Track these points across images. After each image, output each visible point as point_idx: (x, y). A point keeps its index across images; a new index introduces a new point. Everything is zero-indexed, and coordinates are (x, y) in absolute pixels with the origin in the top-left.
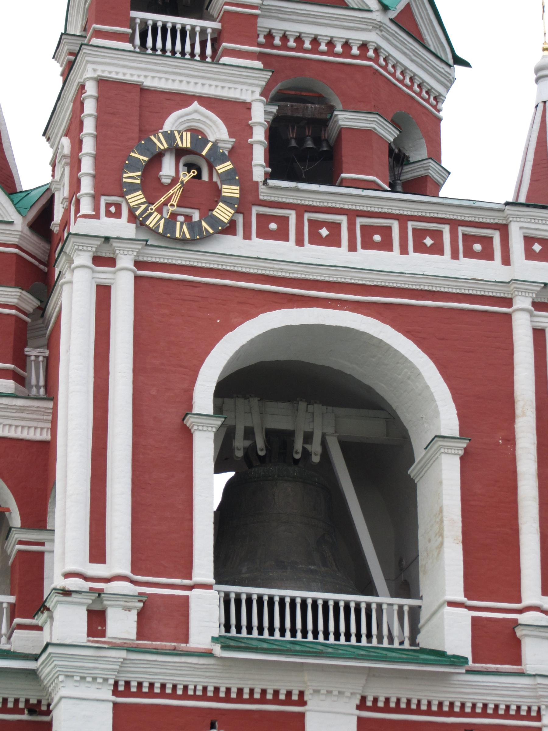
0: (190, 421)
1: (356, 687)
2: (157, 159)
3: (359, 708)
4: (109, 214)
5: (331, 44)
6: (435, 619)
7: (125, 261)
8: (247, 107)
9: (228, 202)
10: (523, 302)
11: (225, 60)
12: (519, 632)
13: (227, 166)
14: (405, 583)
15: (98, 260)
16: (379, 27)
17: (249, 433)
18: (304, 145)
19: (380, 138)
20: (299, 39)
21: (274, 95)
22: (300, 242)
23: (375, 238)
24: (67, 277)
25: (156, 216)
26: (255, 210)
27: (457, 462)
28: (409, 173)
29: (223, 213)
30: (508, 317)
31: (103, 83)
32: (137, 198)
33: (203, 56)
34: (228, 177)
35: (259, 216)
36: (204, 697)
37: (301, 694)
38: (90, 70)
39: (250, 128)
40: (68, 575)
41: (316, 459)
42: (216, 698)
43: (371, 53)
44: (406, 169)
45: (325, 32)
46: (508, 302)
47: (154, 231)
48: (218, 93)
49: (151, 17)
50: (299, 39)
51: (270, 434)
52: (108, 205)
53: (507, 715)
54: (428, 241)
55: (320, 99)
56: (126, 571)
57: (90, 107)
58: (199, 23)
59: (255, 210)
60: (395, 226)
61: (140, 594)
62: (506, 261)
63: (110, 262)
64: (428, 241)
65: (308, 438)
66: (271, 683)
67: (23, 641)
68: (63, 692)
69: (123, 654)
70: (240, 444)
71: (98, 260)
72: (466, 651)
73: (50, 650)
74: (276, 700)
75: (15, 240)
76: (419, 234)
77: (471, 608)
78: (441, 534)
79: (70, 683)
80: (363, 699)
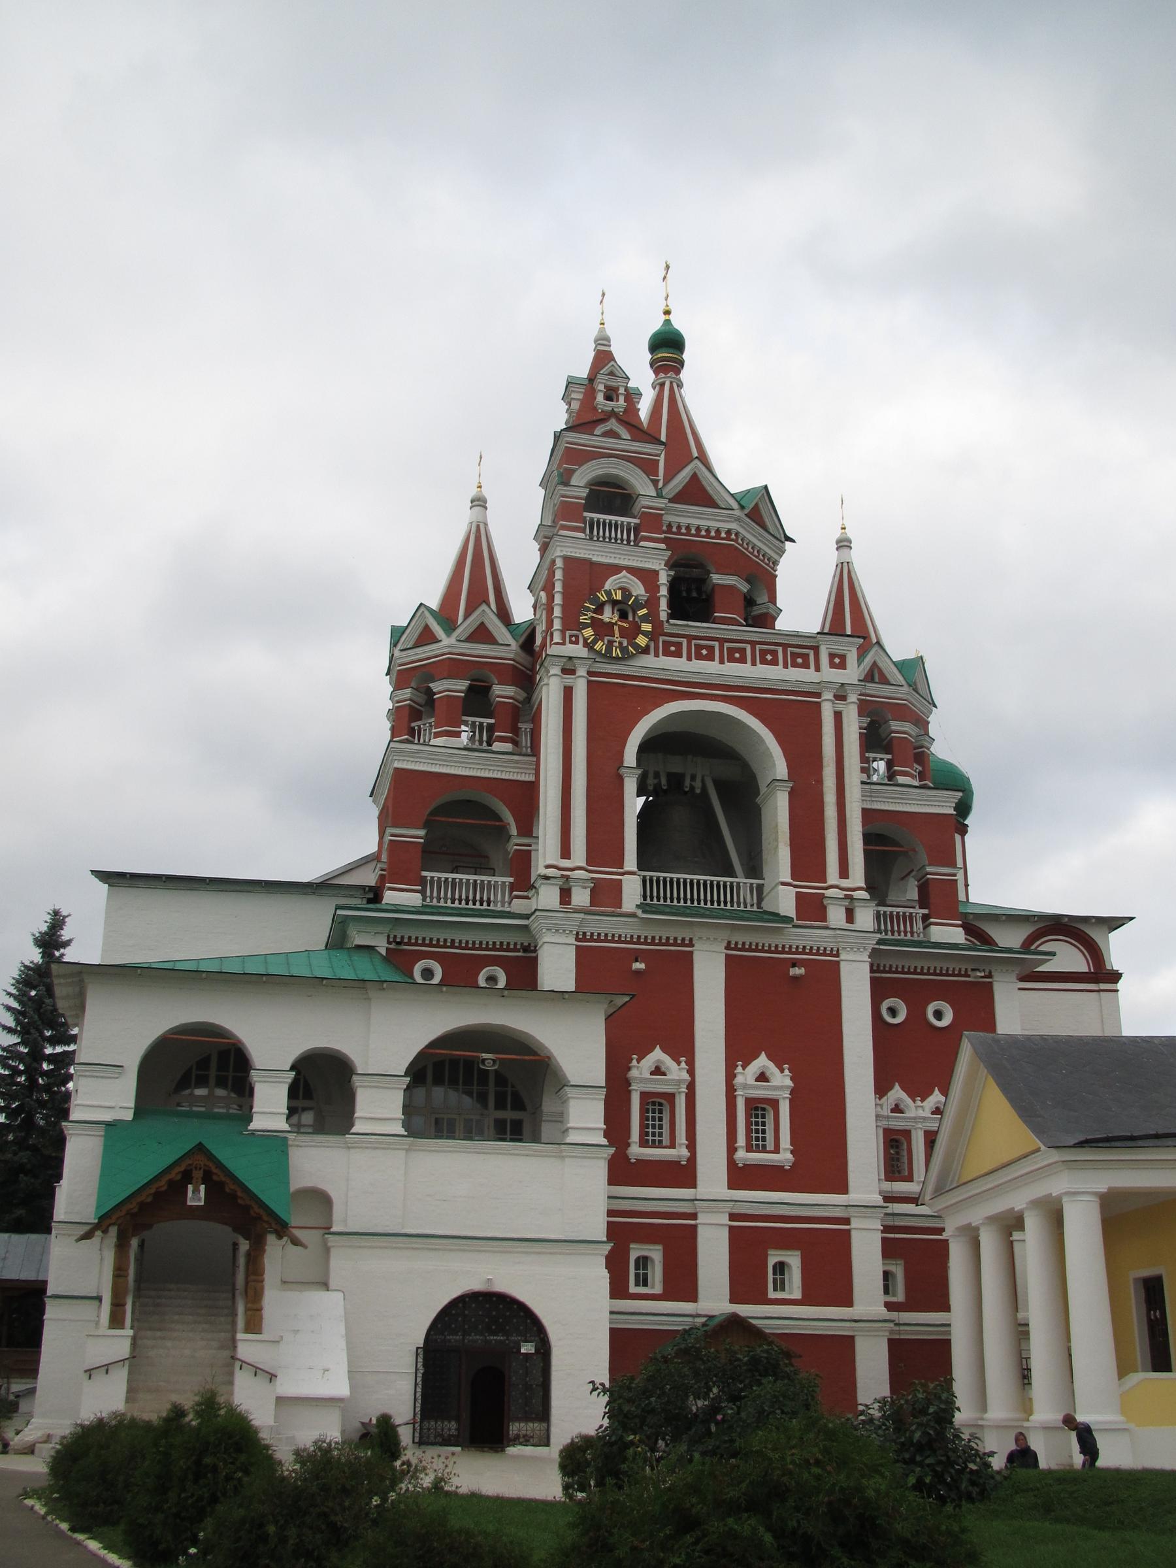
0: (622, 771)
1: (725, 935)
3: (726, 948)
4: (571, 642)
5: (708, 531)
6: (773, 893)
7: (582, 672)
8: (656, 573)
9: (645, 633)
10: (828, 695)
11: (642, 543)
12: (825, 902)
13: (644, 611)
14: (754, 868)
15: (565, 671)
16: (738, 520)
17: (657, 775)
18: (691, 596)
19: (738, 590)
20: (688, 528)
21: (671, 565)
22: (689, 659)
24: (546, 681)
25: (600, 643)
26: (661, 639)
27: (786, 795)
28: (757, 611)
29: (642, 641)
30: (819, 704)
31: (566, 559)
32: (588, 632)
33: (629, 541)
34: (645, 619)
35: (664, 642)
37: (691, 940)
38: (559, 551)
39: (658, 587)
40: (548, 867)
41: (698, 791)
43: (733, 536)
44: (755, 608)
45: (704, 523)
46: (818, 695)
47: (599, 653)
48: (637, 564)
49: (595, 516)
50: (688, 528)
51: (670, 776)
52: (571, 636)
54: (769, 657)
55: (701, 566)
56: (584, 864)
57: (559, 575)
58: (626, 520)
59: (661, 639)
60: (748, 648)
61: (593, 878)
62: (818, 669)
63: (572, 672)
64: (769, 657)
65: (693, 778)
66: (672, 933)
67: (518, 906)
68: (546, 939)
69: (582, 916)
70: (651, 781)
71: (565, 671)
72: (792, 913)
73: (537, 913)
74: (675, 944)
75: (511, 656)
76: (763, 653)
78: (776, 840)
79: (549, 933)
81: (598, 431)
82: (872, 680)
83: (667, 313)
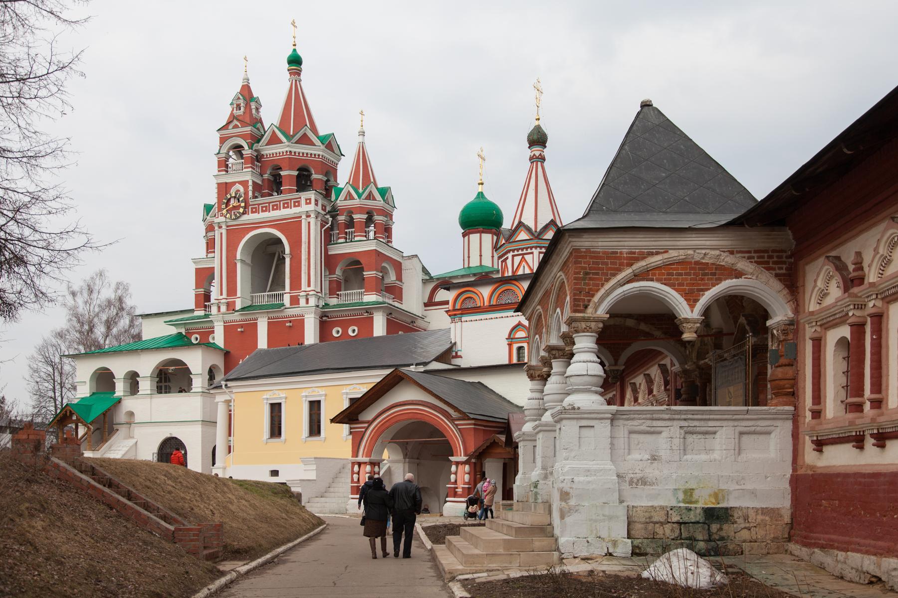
2: (229, 200)
10: (304, 217)
23: (276, 207)
45: (278, 151)
81: (231, 126)
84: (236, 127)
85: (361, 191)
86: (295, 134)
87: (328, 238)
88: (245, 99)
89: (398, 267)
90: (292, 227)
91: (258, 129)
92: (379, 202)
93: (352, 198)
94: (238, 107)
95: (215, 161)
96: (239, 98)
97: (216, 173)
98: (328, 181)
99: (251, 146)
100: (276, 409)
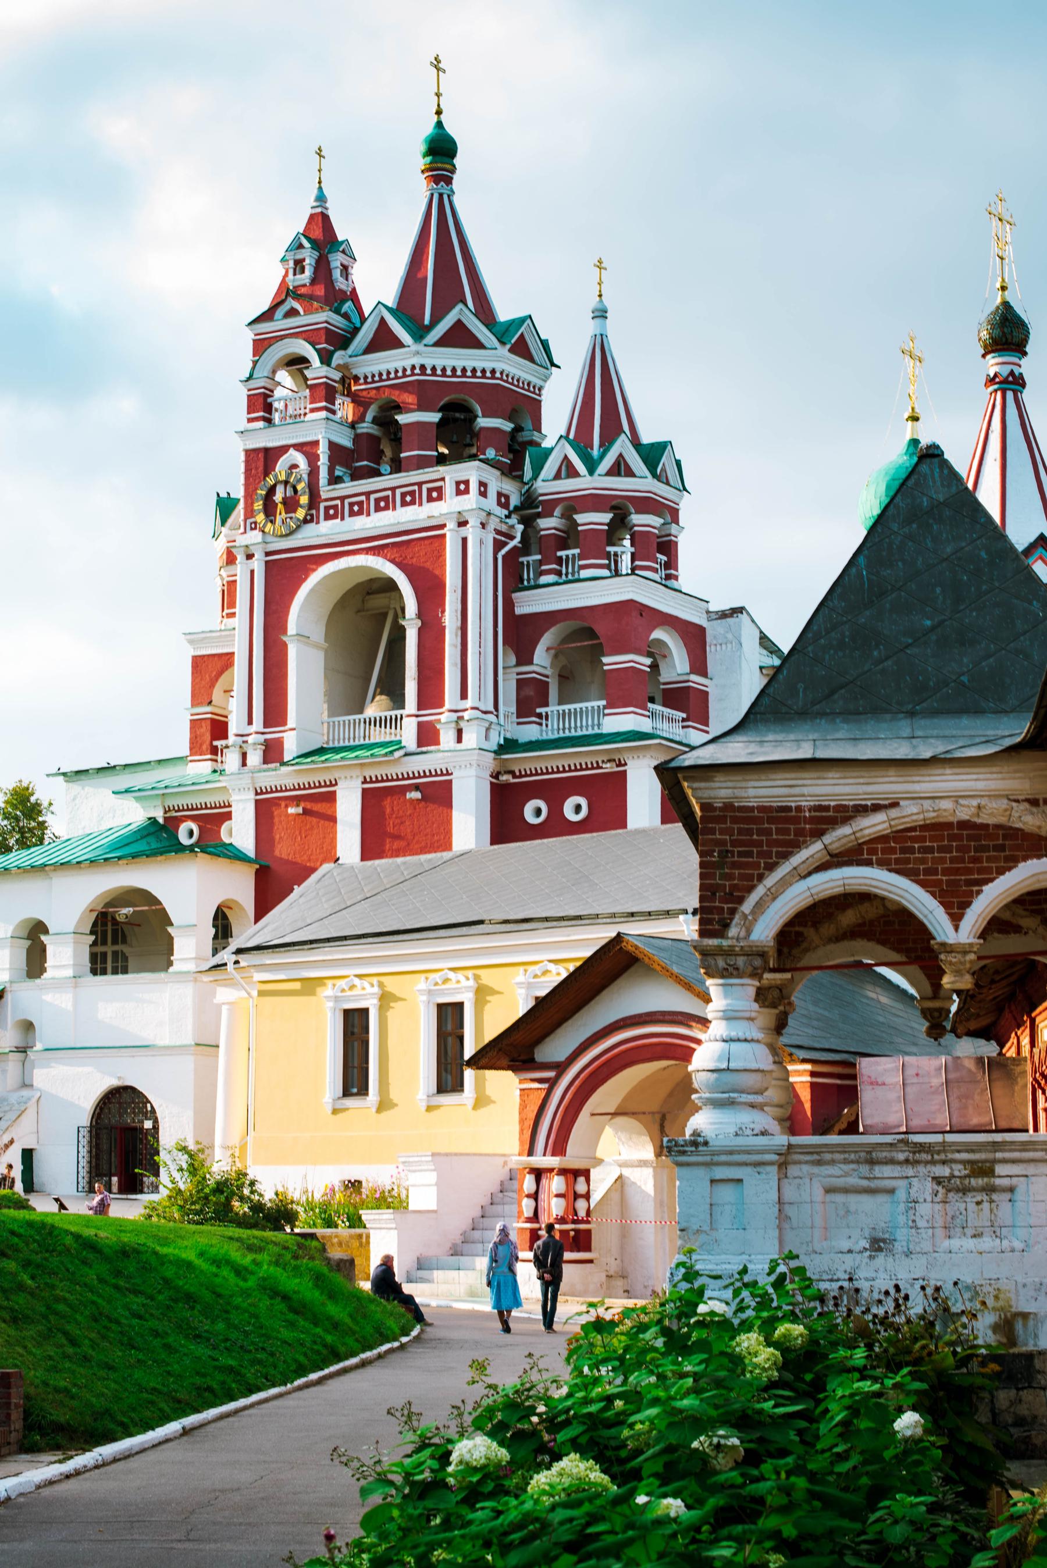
2: (272, 490)
4: (252, 529)
16: (418, 353)
23: (384, 504)
32: (260, 518)
36: (294, 789)
42: (300, 789)
53: (437, 775)
59: (322, 505)
77: (417, 716)
80: (365, 778)
81: (280, 313)
82: (568, 476)
83: (439, 113)
84: (292, 313)
85: (595, 452)
86: (435, 320)
87: (513, 576)
88: (316, 244)
89: (694, 638)
90: (419, 554)
91: (346, 316)
92: (642, 483)
93: (573, 473)
94: (299, 264)
95: (242, 395)
96: (301, 246)
97: (244, 425)
98: (518, 429)
99: (326, 358)
100: (355, 1025)
